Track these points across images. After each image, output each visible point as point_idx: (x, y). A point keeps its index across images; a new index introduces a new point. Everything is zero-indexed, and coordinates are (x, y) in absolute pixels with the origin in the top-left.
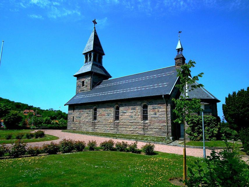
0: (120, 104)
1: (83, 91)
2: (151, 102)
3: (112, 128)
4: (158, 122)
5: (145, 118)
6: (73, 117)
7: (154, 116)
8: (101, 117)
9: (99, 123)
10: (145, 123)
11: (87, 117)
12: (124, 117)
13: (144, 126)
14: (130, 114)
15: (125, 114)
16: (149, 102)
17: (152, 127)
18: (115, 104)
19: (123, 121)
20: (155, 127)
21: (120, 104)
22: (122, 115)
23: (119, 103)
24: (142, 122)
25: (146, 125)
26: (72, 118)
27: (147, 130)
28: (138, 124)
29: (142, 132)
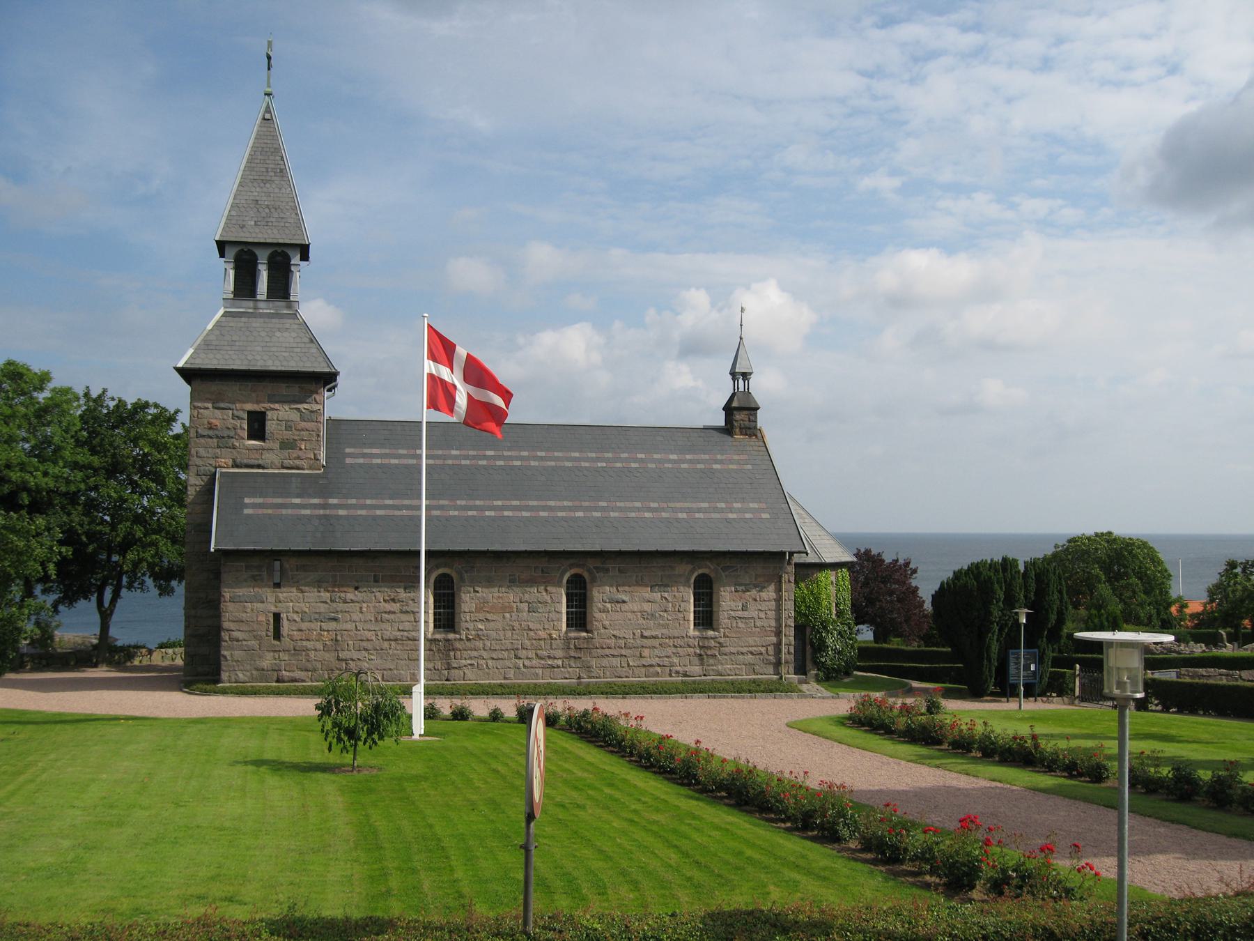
0: (596, 568)
1: (259, 466)
2: (732, 567)
3: (560, 662)
4: (752, 634)
5: (706, 619)
6: (277, 617)
7: (740, 614)
8: (489, 616)
9: (480, 644)
10: (707, 638)
11: (392, 617)
12: (616, 616)
13: (701, 647)
14: (647, 607)
15: (624, 607)
16: (724, 569)
17: (733, 650)
18: (571, 566)
19: (615, 633)
20: (744, 650)
21: (596, 568)
22: (605, 611)
23: (591, 563)
24: (697, 633)
25: (712, 643)
26: (262, 618)
27: (712, 661)
28: (677, 642)
29: (696, 669)
